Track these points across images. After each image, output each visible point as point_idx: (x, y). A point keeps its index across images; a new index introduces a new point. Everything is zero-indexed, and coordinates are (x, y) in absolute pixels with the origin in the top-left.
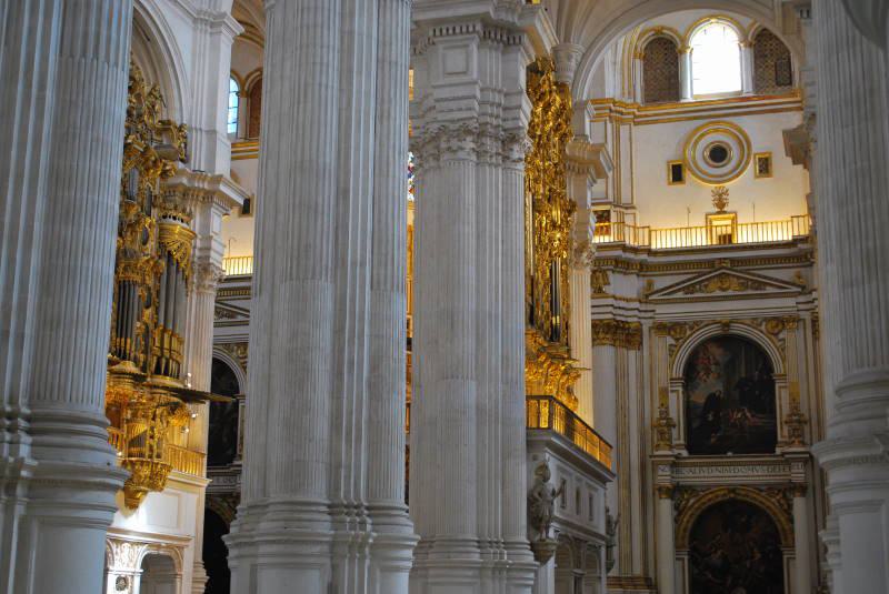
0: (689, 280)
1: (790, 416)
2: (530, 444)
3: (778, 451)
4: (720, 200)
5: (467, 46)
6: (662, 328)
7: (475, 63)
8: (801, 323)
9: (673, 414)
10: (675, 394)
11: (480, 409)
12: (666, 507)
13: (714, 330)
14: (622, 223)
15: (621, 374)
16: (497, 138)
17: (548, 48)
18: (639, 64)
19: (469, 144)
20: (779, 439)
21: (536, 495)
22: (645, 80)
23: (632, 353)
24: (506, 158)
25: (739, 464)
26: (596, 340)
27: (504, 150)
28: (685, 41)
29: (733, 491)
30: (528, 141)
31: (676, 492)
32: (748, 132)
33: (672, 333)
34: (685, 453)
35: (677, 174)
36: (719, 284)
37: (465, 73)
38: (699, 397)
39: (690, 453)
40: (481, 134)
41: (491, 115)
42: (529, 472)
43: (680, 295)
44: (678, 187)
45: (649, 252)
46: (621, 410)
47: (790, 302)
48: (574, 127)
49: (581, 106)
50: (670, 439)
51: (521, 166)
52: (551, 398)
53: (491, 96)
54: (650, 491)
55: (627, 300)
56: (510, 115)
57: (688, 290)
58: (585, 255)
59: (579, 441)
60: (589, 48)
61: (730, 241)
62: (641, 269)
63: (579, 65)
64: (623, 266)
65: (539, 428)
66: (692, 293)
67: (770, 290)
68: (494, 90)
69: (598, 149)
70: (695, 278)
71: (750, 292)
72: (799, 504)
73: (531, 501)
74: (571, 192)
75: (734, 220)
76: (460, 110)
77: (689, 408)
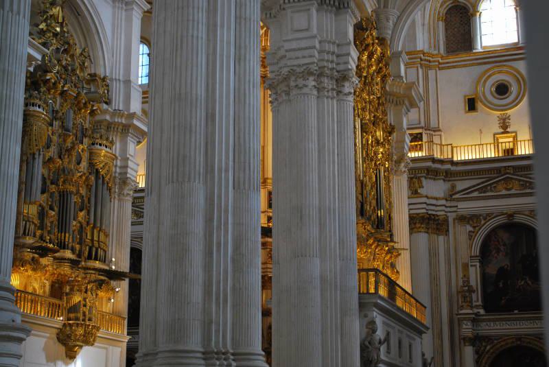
0: (483, 183)
2: (362, 305)
4: (504, 123)
5: (309, 10)
6: (462, 219)
9: (473, 283)
10: (474, 268)
11: (323, 279)
12: (469, 352)
13: (501, 220)
14: (431, 142)
15: (433, 253)
16: (332, 78)
17: (370, 11)
18: (441, 25)
19: (311, 82)
21: (367, 343)
22: (446, 37)
23: (441, 238)
24: (339, 92)
26: (412, 229)
27: (337, 87)
29: (519, 339)
30: (355, 80)
31: (476, 340)
34: (482, 311)
35: (471, 105)
36: (505, 186)
37: (307, 30)
38: (492, 270)
40: (321, 75)
41: (328, 61)
42: (361, 326)
43: (475, 194)
44: (474, 114)
45: (452, 162)
46: (434, 280)
48: (391, 69)
49: (397, 55)
50: (471, 302)
51: (351, 98)
52: (376, 271)
53: (327, 47)
54: (457, 340)
55: (436, 199)
56: (342, 60)
58: (403, 165)
59: (399, 302)
61: (512, 153)
62: (446, 176)
63: (395, 25)
64: (432, 174)
65: (368, 293)
66: (485, 192)
68: (329, 42)
69: (410, 86)
70: (483, 183)
73: (364, 348)
74: (391, 119)
75: (515, 138)
76: (304, 57)
77: (484, 277)
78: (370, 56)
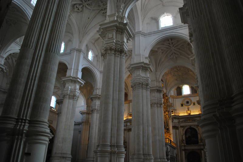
6: (181, 127)
7: (156, 95)
9: (184, 139)
12: (183, 152)
13: (189, 127)
14: (175, 112)
15: (176, 134)
19: (156, 105)
23: (177, 131)
26: (173, 129)
28: (182, 88)
30: (163, 104)
32: (191, 99)
34: (186, 144)
35: (182, 105)
38: (187, 136)
39: (186, 143)
40: (157, 104)
45: (179, 116)
46: (176, 138)
48: (168, 101)
49: (169, 98)
51: (163, 108)
52: (168, 139)
53: (158, 99)
55: (177, 123)
57: (185, 121)
59: (172, 144)
60: (170, 90)
63: (168, 93)
69: (172, 104)
71: (193, 121)
72: (202, 152)
74: (168, 110)
75: (190, 111)
78: (165, 99)
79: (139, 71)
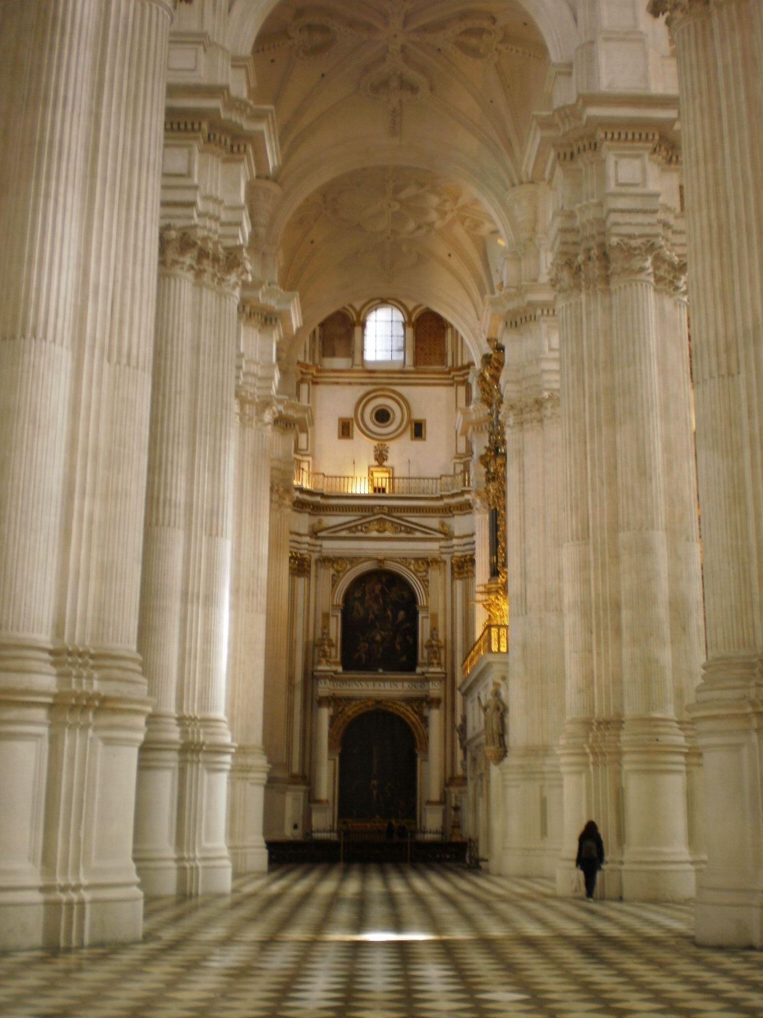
0: (354, 521)
1: (429, 641)
3: (419, 670)
6: (326, 561)
8: (442, 565)
10: (335, 618)
12: (325, 714)
13: (366, 566)
20: (420, 660)
25: (384, 680)
33: (335, 566)
34: (340, 669)
35: (345, 430)
43: (344, 534)
47: (434, 546)
57: (349, 529)
66: (354, 532)
67: (418, 535)
71: (403, 535)
72: (435, 716)
79: (191, 146)
